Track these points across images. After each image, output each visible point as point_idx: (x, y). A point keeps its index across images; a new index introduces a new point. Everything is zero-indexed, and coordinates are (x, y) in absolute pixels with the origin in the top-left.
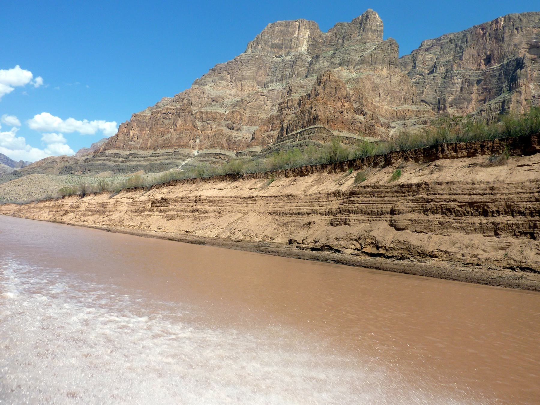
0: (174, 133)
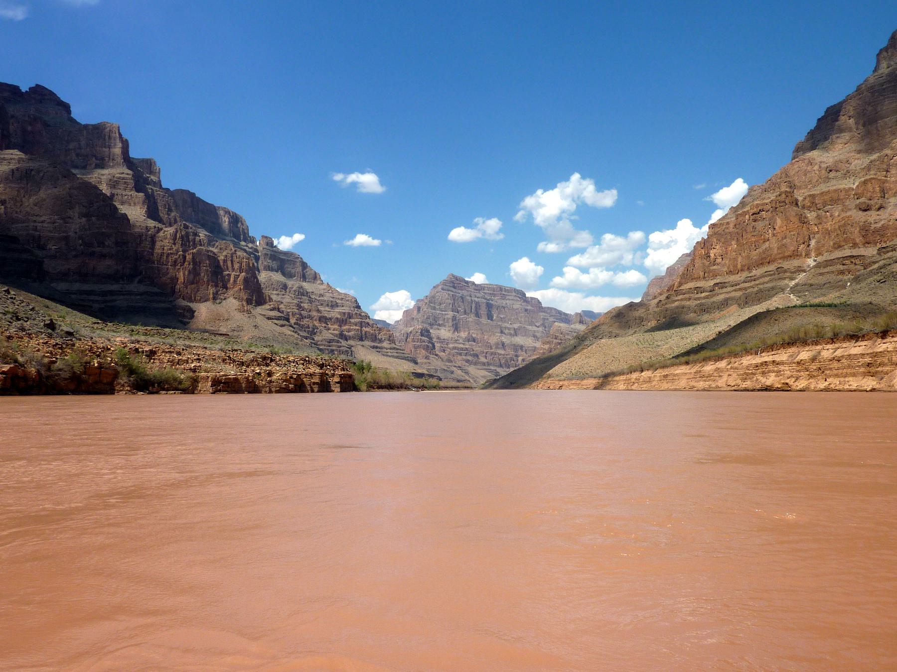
0: (773, 240)
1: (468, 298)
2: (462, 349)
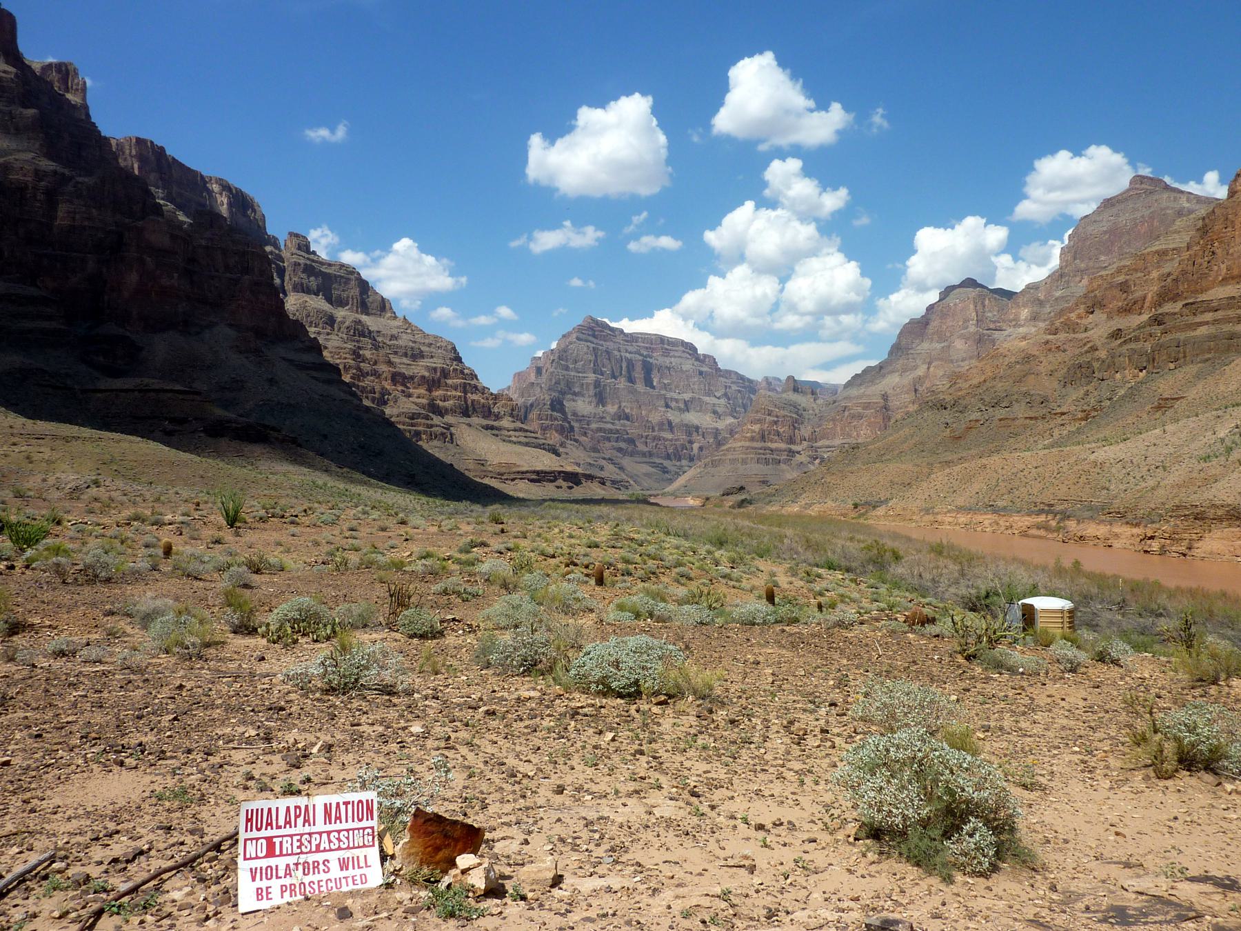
1: (616, 353)
2: (611, 431)
